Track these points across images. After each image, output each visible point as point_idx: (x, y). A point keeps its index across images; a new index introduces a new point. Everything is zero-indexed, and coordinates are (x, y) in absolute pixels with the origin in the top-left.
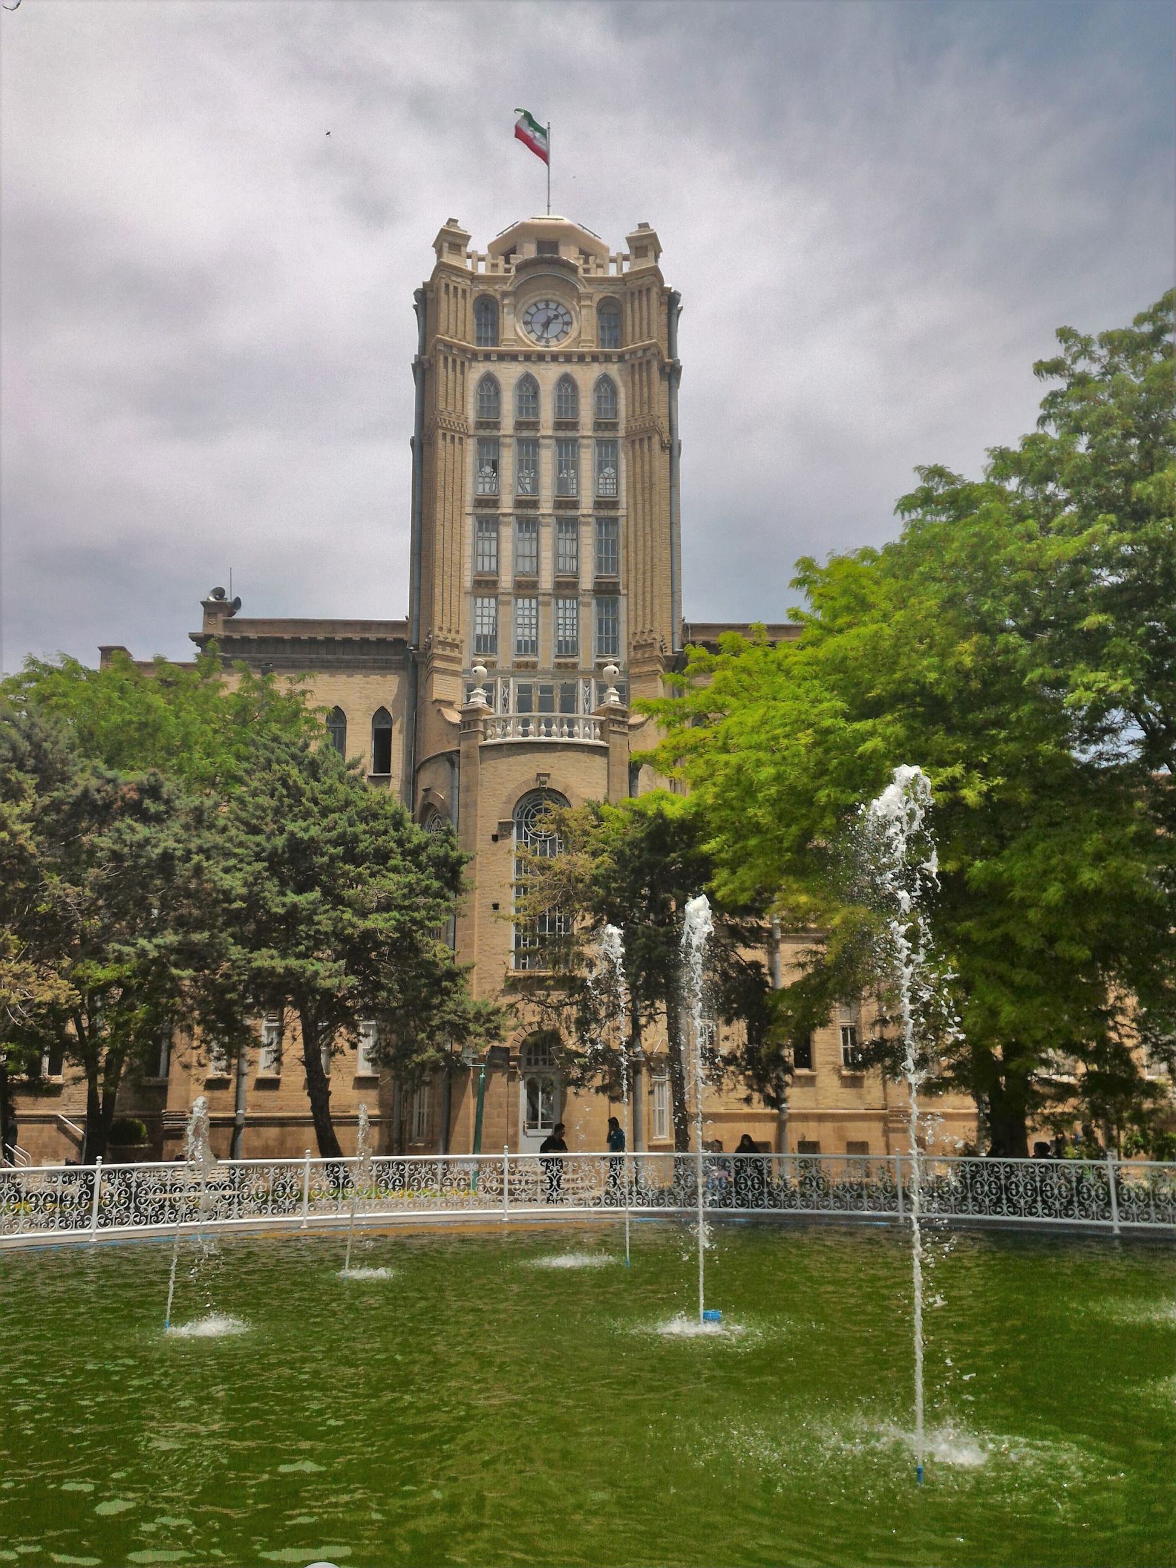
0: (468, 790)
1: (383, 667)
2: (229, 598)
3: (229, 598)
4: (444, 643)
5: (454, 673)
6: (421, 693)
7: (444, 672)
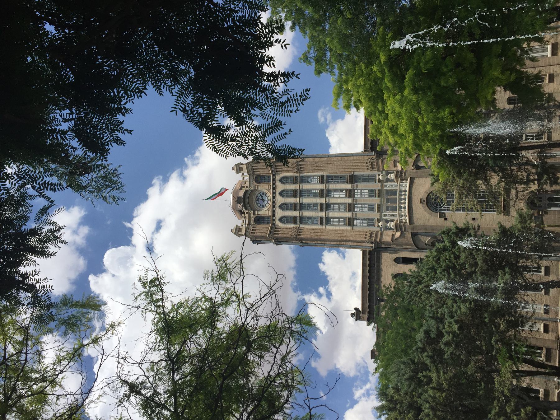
0: (426, 229)
1: (379, 259)
2: (354, 311)
3: (354, 311)
4: (371, 237)
5: (382, 234)
7: (381, 237)
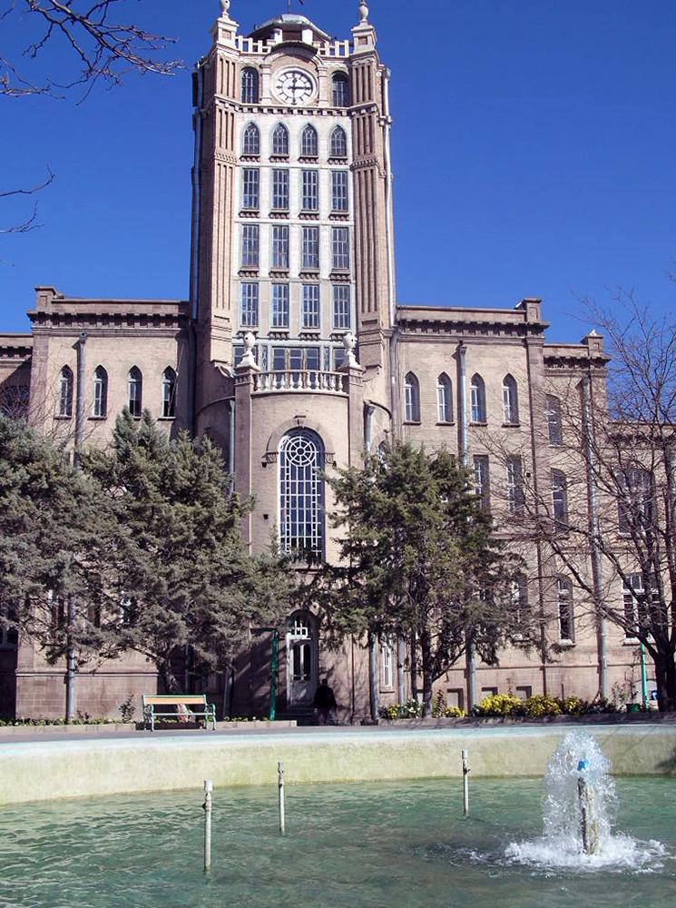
5: (227, 340)
6: (200, 356)
7: (219, 338)
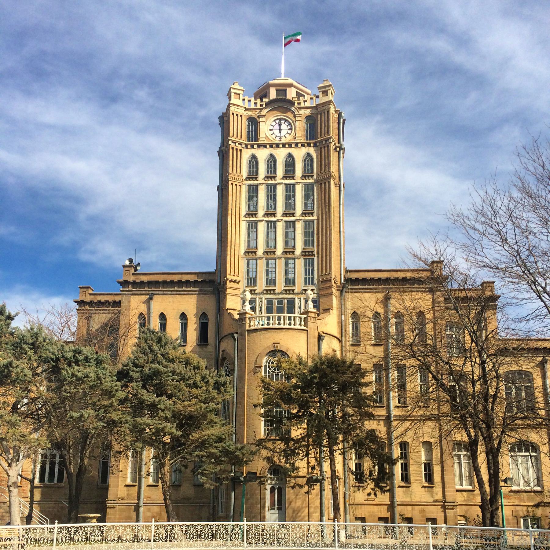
4: (231, 281)
5: (237, 295)
7: (232, 295)
